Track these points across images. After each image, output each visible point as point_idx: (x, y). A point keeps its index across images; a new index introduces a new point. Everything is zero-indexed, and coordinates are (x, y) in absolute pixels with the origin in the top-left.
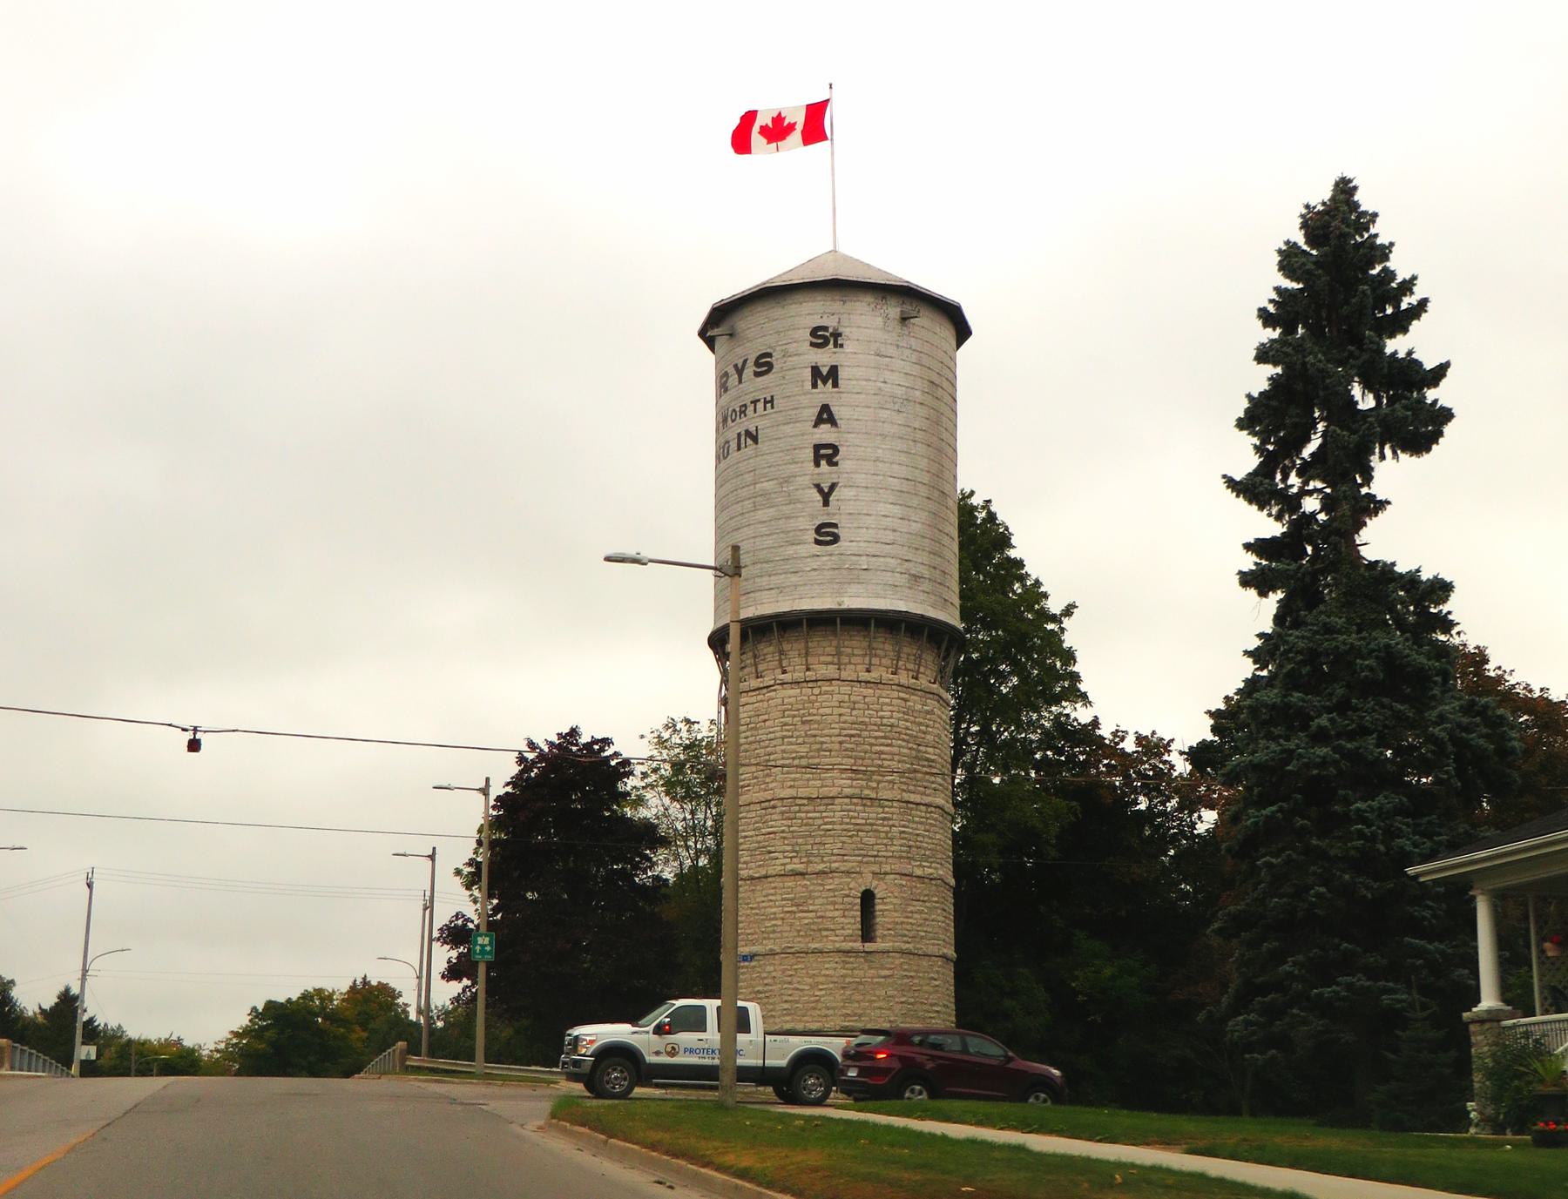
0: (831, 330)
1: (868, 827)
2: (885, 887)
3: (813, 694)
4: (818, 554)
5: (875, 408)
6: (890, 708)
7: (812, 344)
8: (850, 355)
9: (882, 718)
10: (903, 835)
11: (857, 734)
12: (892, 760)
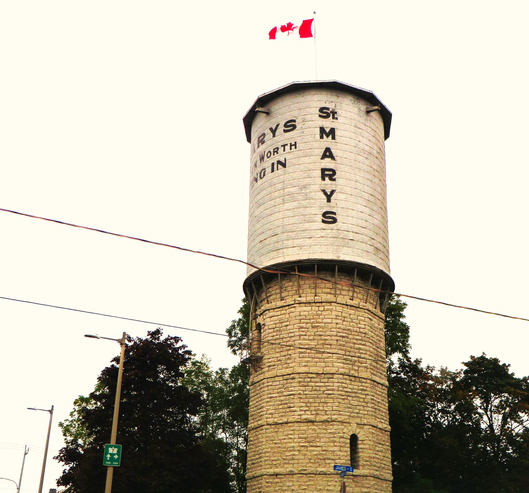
0: (331, 110)
1: (353, 394)
2: (364, 433)
3: (319, 310)
4: (324, 228)
5: (355, 154)
6: (364, 323)
7: (320, 116)
8: (341, 124)
9: (360, 328)
10: (373, 401)
11: (346, 336)
12: (366, 354)
